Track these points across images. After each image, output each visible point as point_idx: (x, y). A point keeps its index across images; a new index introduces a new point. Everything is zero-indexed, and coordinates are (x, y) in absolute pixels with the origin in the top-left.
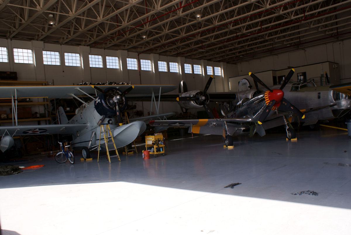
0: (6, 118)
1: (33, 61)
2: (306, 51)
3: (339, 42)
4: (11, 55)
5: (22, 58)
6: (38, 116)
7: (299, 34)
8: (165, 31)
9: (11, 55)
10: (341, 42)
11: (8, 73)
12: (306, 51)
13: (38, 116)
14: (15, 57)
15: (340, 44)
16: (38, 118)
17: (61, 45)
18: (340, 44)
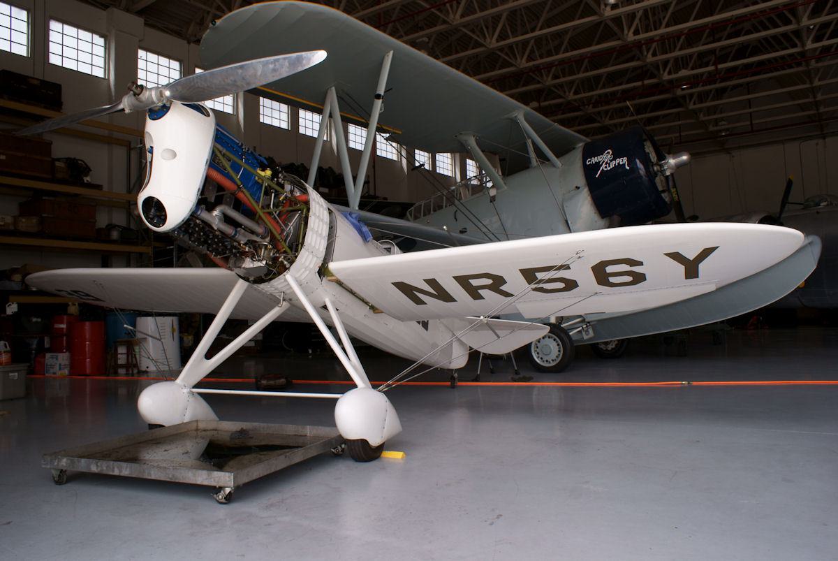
0: (12, 228)
1: (107, 69)
2: (733, 157)
3: (815, 142)
4: (39, 39)
5: (73, 53)
6: (115, 235)
7: (750, 108)
8: (490, 43)
9: (39, 39)
10: (821, 141)
11: (36, 82)
12: (733, 157)
13: (115, 235)
14: (53, 48)
15: (817, 144)
16: (114, 242)
17: (189, 43)
18: (817, 144)
